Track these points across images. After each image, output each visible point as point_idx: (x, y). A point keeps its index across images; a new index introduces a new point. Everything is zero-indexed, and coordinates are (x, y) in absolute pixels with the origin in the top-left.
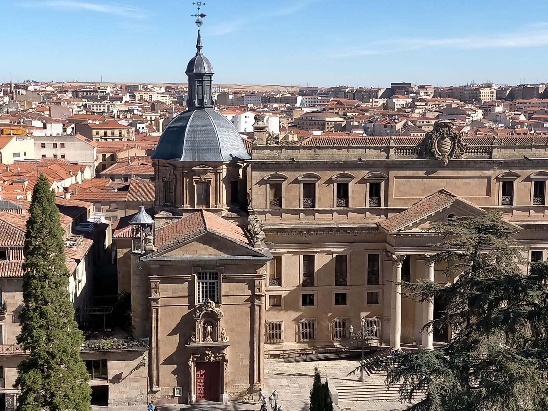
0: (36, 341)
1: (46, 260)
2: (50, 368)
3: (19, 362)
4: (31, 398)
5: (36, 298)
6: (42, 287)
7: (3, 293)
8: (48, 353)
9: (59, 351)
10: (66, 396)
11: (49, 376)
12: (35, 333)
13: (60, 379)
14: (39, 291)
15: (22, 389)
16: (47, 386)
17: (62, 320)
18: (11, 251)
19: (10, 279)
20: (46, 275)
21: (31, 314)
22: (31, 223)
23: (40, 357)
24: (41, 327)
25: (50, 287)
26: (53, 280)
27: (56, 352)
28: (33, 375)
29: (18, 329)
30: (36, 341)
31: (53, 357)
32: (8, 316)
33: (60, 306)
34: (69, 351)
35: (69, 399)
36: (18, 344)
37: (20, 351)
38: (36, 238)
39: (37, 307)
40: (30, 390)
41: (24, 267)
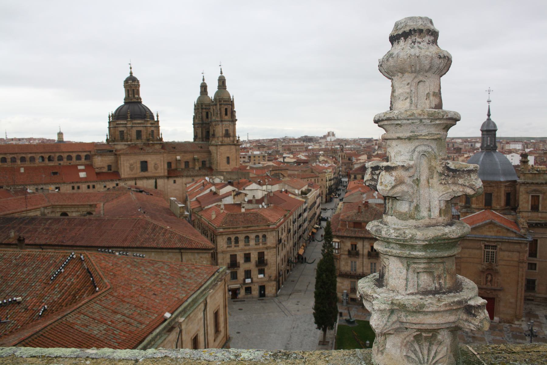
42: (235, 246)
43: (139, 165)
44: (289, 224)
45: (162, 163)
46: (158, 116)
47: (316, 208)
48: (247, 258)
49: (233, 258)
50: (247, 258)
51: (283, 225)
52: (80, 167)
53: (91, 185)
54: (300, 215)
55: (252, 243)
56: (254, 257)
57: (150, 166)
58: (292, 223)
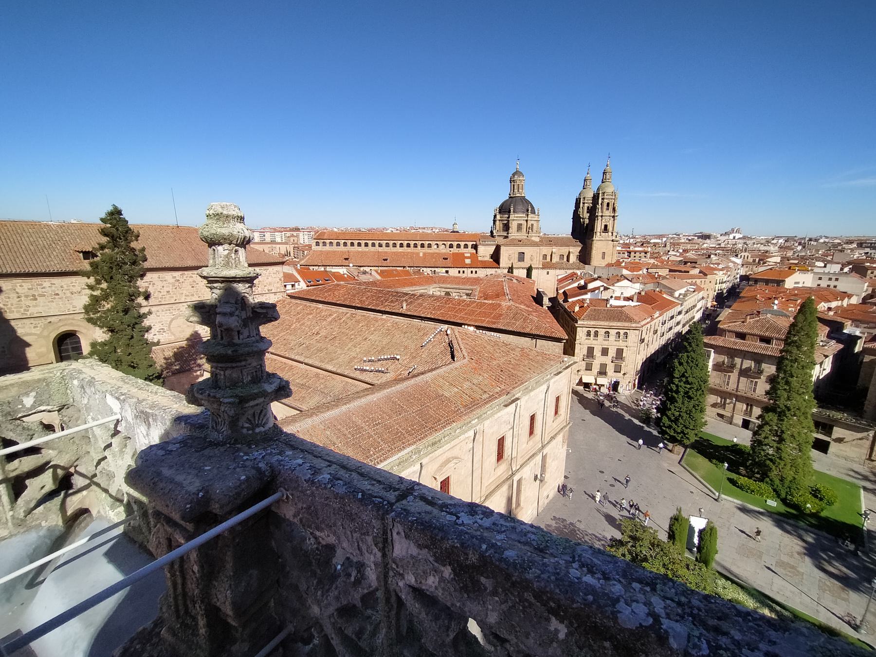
0: (778, 397)
1: (798, 350)
2: (785, 415)
3: (764, 405)
4: (767, 428)
5: (785, 372)
6: (792, 366)
7: (763, 364)
8: (785, 406)
9: (794, 408)
10: (792, 436)
11: (783, 420)
12: (779, 392)
13: (791, 425)
14: (788, 368)
15: (762, 422)
16: (779, 425)
17: (802, 390)
18: (775, 340)
19: (770, 357)
20: (796, 359)
21: (779, 380)
22: (793, 326)
23: (779, 408)
24: (785, 390)
25: (798, 367)
26: (802, 363)
27: (792, 407)
28: (771, 417)
29: (768, 387)
30: (778, 397)
31: (789, 410)
32: (763, 378)
33: (803, 381)
34: (803, 410)
35: (794, 438)
36: (765, 395)
37: (766, 400)
38: (794, 335)
39: (784, 378)
40: (767, 423)
41: (781, 351)
42: (594, 339)
43: (517, 256)
44: (657, 324)
45: (538, 255)
46: (538, 211)
47: (695, 312)
48: (605, 352)
49: (591, 351)
50: (605, 352)
51: (650, 324)
52: (466, 255)
53: (474, 270)
54: (672, 317)
55: (612, 338)
56: (612, 353)
57: (527, 257)
58: (661, 323)
